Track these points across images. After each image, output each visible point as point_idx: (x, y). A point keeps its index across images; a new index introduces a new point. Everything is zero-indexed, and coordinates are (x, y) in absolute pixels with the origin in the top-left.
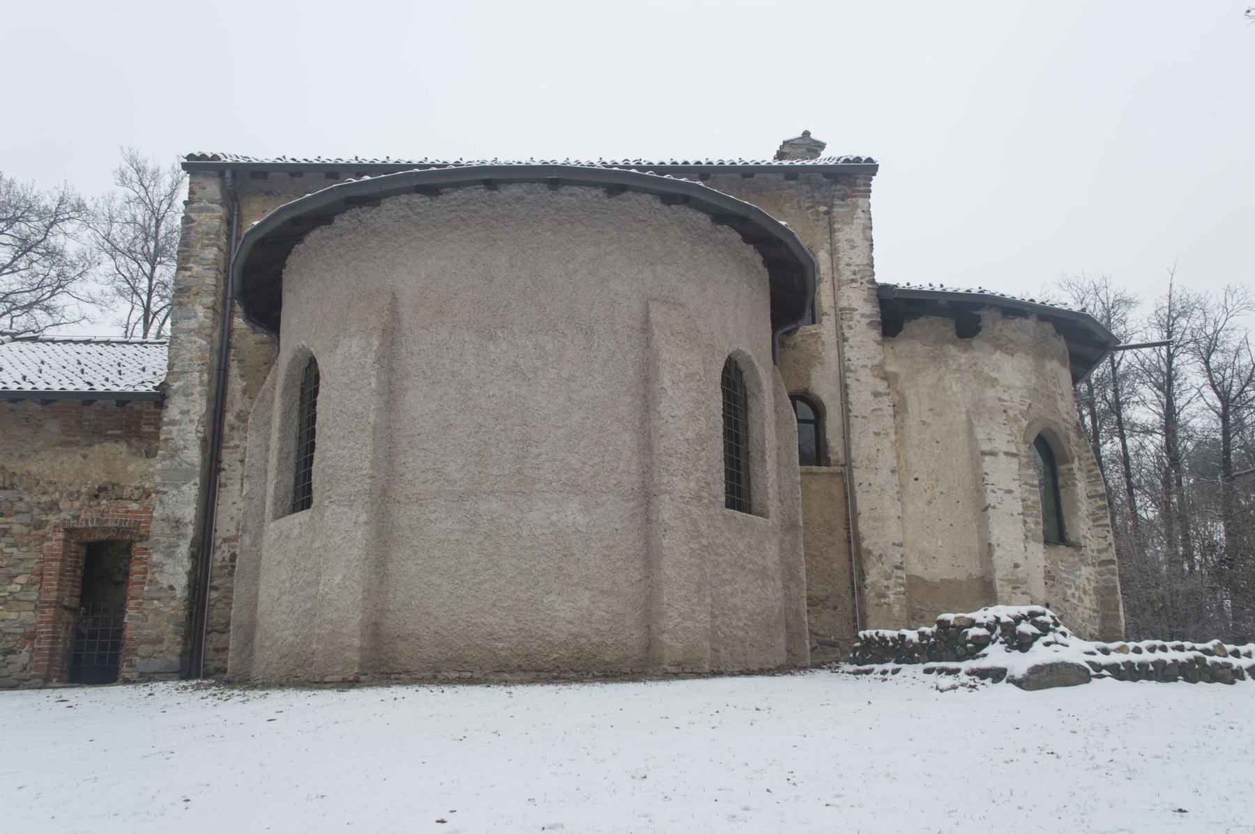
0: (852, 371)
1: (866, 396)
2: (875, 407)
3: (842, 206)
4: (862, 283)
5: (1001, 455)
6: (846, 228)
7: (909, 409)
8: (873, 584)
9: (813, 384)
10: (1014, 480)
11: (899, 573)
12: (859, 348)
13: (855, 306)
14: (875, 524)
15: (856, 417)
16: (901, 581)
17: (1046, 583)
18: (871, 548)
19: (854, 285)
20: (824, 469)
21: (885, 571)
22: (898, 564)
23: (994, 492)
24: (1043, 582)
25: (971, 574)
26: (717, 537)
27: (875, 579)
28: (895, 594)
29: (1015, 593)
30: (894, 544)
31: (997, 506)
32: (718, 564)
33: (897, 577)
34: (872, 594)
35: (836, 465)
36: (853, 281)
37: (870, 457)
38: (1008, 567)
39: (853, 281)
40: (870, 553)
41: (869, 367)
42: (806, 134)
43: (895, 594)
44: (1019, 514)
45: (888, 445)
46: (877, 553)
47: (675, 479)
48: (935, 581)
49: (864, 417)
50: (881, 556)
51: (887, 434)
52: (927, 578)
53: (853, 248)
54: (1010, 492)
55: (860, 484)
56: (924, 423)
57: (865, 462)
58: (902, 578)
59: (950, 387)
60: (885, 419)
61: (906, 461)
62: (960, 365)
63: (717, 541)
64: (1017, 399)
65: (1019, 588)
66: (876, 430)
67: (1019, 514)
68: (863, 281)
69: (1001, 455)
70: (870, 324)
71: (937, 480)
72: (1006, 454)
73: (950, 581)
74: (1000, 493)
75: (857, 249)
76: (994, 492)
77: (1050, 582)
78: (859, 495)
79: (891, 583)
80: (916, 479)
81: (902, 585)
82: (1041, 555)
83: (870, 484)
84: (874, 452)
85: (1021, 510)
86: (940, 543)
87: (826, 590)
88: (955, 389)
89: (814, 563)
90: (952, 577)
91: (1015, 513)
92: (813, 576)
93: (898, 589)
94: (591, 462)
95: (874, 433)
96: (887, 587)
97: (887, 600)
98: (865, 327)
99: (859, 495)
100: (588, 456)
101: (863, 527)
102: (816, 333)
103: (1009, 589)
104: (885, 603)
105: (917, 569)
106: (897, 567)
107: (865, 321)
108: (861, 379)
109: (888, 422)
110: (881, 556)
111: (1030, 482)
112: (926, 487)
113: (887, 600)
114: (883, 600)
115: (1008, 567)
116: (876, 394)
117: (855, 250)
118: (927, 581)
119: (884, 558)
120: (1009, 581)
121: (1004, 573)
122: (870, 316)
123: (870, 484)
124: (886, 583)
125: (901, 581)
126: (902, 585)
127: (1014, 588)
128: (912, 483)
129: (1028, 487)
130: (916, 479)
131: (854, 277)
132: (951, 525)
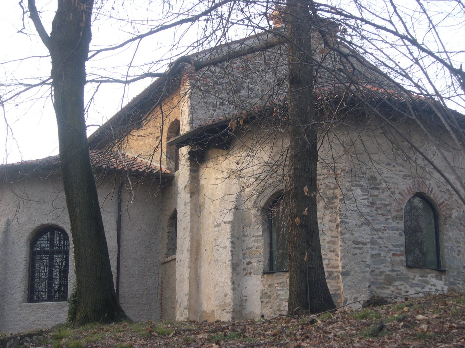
17: (262, 302)
26: (16, 317)
44: (229, 261)
63: (16, 319)
65: (225, 309)
69: (223, 224)
74: (221, 250)
77: (265, 300)
82: (259, 283)
91: (227, 261)
103: (220, 312)
106: (185, 309)
111: (256, 234)
116: (185, 204)
127: (223, 310)
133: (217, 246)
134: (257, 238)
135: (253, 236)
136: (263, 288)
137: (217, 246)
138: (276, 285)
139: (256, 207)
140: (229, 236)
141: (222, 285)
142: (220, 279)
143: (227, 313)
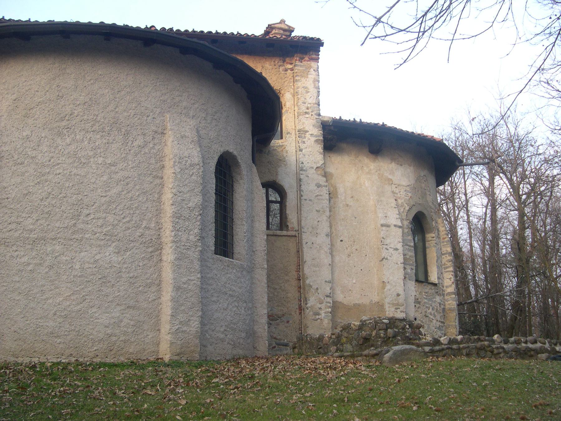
0: (304, 170)
1: (312, 187)
2: (318, 194)
3: (301, 66)
4: (312, 115)
5: (392, 227)
6: (303, 80)
7: (339, 196)
8: (312, 307)
9: (279, 177)
10: (400, 242)
11: (329, 300)
12: (309, 155)
13: (307, 129)
14: (314, 268)
15: (306, 200)
16: (329, 305)
17: (415, 306)
18: (311, 284)
19: (307, 116)
20: (284, 233)
21: (320, 299)
22: (328, 294)
23: (387, 250)
24: (414, 305)
25: (372, 301)
27: (312, 304)
28: (325, 313)
29: (397, 312)
30: (326, 282)
31: (389, 258)
32: (208, 291)
33: (327, 302)
34: (311, 313)
35: (292, 231)
36: (306, 113)
37: (313, 226)
38: (393, 296)
39: (306, 113)
40: (311, 286)
41: (315, 168)
42: (283, 21)
43: (325, 313)
44: (401, 263)
45: (325, 218)
46: (315, 287)
47: (180, 233)
48: (350, 305)
49: (310, 200)
50: (317, 289)
51: (324, 212)
52: (345, 303)
53: (307, 92)
54: (397, 249)
55: (307, 243)
56: (347, 205)
57: (310, 229)
58: (330, 303)
59: (364, 183)
60: (324, 202)
61: (336, 230)
62: (371, 170)
64: (403, 193)
65: (399, 308)
66: (317, 209)
67: (401, 263)
68: (313, 113)
69: (392, 227)
70: (316, 141)
71: (354, 242)
72: (395, 226)
73: (359, 305)
74: (391, 250)
75: (309, 93)
76: (387, 250)
77: (418, 305)
78: (305, 249)
79: (323, 306)
80: (342, 241)
81: (330, 307)
82: (413, 288)
83: (313, 243)
84: (316, 222)
85: (402, 261)
86: (354, 281)
87: (283, 310)
88: (367, 184)
89: (276, 294)
90: (360, 302)
91: (399, 263)
92: (275, 302)
93: (327, 310)
94: (125, 220)
95: (317, 210)
96: (320, 308)
97: (320, 317)
98: (313, 143)
99: (305, 250)
100: (122, 216)
101: (307, 270)
102: (283, 145)
103: (393, 309)
104: (319, 319)
105: (340, 297)
106: (327, 296)
107: (313, 139)
108: (310, 176)
109: (326, 203)
110: (317, 289)
111: (409, 244)
112: (348, 246)
113: (320, 317)
114: (317, 317)
115: (393, 296)
117: (308, 94)
118: (345, 305)
119: (319, 291)
120: (393, 304)
121: (391, 299)
122: (316, 136)
123: (313, 243)
124: (320, 306)
125: (329, 305)
126: (330, 307)
127: (397, 309)
128: (339, 242)
129: (407, 247)
130: (342, 241)
131: (307, 111)
132: (361, 270)
133: (386, 245)
134: (410, 248)
135: (407, 245)
136: (416, 294)
137: (386, 245)
138: (424, 294)
139: (408, 220)
140: (401, 240)
141: (394, 284)
142: (391, 278)
143: (401, 312)
